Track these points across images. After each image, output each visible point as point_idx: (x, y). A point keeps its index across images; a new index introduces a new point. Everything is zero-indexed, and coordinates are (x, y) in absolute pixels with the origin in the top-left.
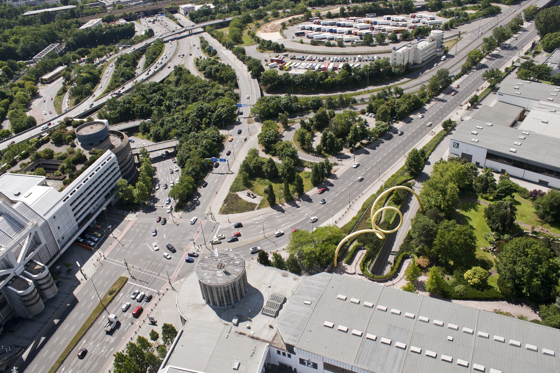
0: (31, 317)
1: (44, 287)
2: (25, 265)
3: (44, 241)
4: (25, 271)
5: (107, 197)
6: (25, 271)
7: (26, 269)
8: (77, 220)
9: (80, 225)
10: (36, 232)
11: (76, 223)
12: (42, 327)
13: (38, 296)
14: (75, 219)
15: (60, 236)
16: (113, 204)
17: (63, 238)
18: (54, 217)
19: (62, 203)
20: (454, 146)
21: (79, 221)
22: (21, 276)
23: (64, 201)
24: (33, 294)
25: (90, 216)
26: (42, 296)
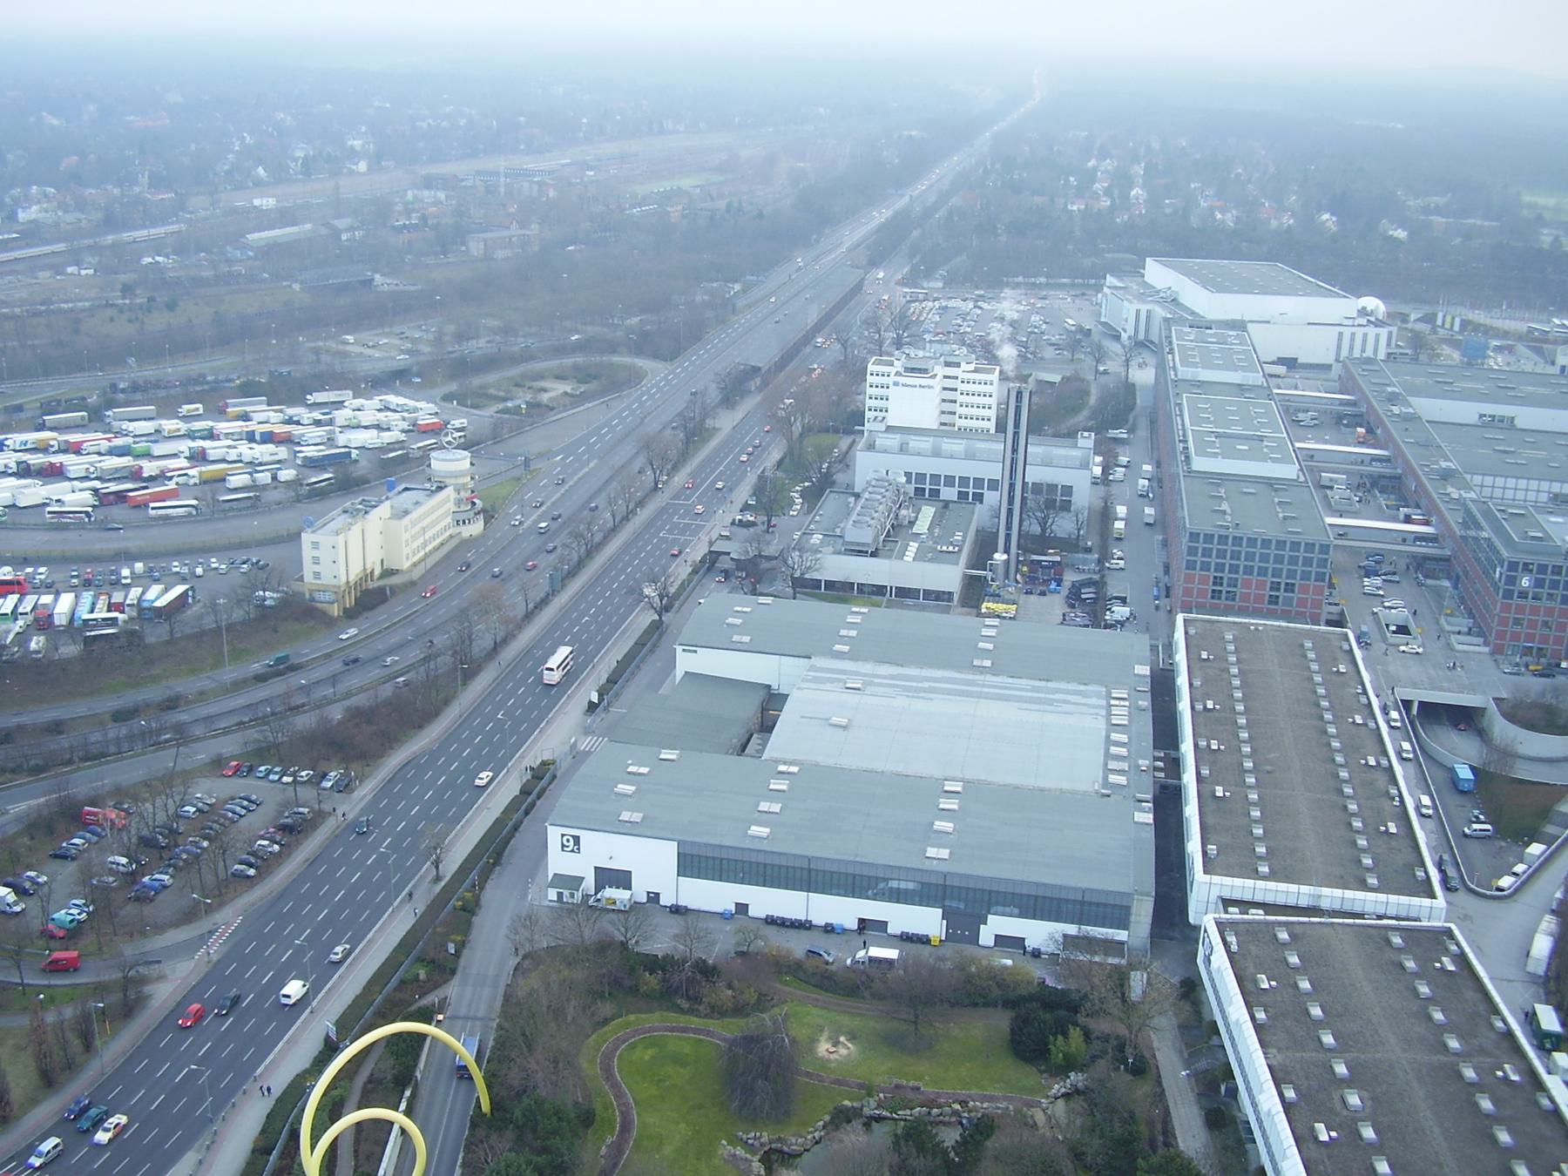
20: (563, 846)
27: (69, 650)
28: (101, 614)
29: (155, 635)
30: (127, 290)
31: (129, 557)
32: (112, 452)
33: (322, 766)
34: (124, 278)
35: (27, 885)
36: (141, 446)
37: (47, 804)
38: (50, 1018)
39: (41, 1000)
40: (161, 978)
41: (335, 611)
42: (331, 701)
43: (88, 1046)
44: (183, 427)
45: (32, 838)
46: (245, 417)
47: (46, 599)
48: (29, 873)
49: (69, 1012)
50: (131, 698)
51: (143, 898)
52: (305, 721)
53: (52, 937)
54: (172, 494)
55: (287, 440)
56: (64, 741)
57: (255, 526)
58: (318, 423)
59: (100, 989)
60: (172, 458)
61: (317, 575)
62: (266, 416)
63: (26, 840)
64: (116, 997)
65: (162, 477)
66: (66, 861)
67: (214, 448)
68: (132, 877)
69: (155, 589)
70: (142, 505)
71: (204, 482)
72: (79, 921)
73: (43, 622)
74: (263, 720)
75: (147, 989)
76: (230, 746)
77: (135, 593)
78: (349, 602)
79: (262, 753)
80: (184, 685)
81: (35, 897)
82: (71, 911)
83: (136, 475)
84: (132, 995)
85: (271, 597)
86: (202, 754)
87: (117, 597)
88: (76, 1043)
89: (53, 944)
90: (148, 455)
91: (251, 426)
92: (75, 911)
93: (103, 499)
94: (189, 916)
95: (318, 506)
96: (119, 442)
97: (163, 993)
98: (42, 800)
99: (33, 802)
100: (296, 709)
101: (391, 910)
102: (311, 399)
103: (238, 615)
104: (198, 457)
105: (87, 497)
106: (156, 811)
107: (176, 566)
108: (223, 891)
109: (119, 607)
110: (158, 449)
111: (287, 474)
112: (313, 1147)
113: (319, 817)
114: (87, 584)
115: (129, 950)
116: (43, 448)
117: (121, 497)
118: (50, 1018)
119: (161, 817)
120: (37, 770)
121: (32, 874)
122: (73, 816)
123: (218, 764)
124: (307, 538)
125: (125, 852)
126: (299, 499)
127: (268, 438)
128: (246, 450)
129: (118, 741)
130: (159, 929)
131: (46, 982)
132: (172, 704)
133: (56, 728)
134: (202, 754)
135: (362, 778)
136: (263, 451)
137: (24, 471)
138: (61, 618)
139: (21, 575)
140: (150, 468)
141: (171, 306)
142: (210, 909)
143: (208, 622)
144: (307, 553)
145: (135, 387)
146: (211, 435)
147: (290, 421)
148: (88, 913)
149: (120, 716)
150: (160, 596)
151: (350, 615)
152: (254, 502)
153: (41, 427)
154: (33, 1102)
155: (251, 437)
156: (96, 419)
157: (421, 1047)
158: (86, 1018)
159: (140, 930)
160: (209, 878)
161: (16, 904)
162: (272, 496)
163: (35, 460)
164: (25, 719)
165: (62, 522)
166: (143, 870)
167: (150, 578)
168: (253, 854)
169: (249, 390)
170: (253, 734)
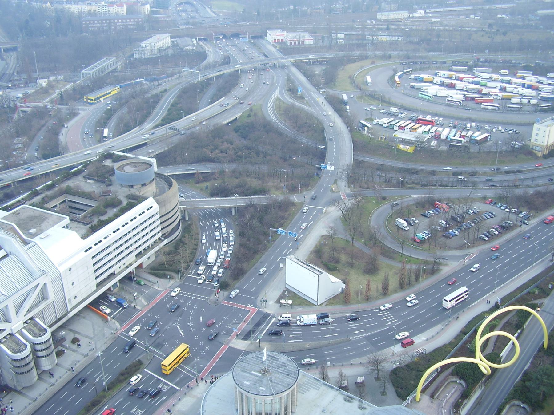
0: (19, 389)
1: (41, 354)
2: (25, 322)
3: (52, 297)
4: (23, 330)
5: (139, 255)
6: (23, 330)
7: (24, 327)
8: (96, 279)
9: (100, 285)
10: (45, 284)
11: (95, 282)
12: (30, 404)
13: (33, 363)
17: (75, 297)
18: (70, 269)
21: (99, 280)
22: (17, 335)
23: (86, 251)
24: (28, 360)
25: (113, 275)
26: (37, 366)
27: (444, 148)
28: (457, 138)
29: (474, 149)
30: (490, 26)
31: (471, 120)
32: (473, 83)
33: (521, 209)
34: (490, 21)
35: (412, 222)
36: (483, 82)
37: (424, 197)
38: (408, 267)
39: (406, 260)
40: (446, 265)
41: (540, 154)
42: (530, 187)
43: (417, 280)
44: (500, 78)
45: (417, 207)
46: (523, 78)
47: (440, 129)
48: (413, 218)
49: (414, 267)
50: (460, 169)
51: (447, 237)
52: (519, 191)
53: (415, 241)
54: (491, 101)
55: (537, 89)
56: (435, 178)
57: (517, 118)
58: (549, 84)
59: (426, 263)
60: (493, 87)
61: (536, 140)
62: (531, 79)
63: (415, 207)
64: (430, 267)
65: (488, 94)
66: (425, 218)
67: (509, 87)
68: (446, 229)
69: (478, 133)
70: (480, 103)
71: (503, 99)
72: (425, 238)
73: (437, 137)
74: (504, 187)
75: (441, 267)
76: (490, 193)
77: (470, 133)
78: (546, 152)
79: (501, 199)
80: (479, 169)
81: (413, 227)
82: (423, 234)
83: (479, 92)
84: (435, 267)
85: (517, 144)
86: (480, 194)
87: (464, 133)
88: (413, 277)
89: (415, 243)
90: (485, 86)
91: (524, 82)
92: (424, 235)
93: (466, 98)
94: (461, 247)
95: (542, 115)
96: (476, 79)
97: (446, 270)
98: (423, 196)
99: (420, 196)
100: (517, 186)
101: (532, 266)
102: (549, 75)
103: (504, 148)
104: (503, 89)
105: (461, 97)
106: (459, 209)
107: (486, 127)
108: (475, 242)
109: (464, 137)
110: (489, 84)
111: (534, 101)
112: (481, 338)
113: (515, 226)
114: (455, 127)
115: (439, 253)
116: (450, 78)
117: (473, 99)
118: (408, 267)
119: (461, 212)
120: (423, 185)
121: (414, 219)
122: (432, 203)
123: (484, 198)
124: (536, 126)
125: (446, 220)
126: (536, 111)
127: (530, 87)
128: (521, 90)
129: (452, 182)
130: (450, 248)
131: (409, 255)
132: (473, 174)
133: (433, 173)
134: (480, 194)
135: (534, 217)
136: (527, 91)
137: (442, 84)
138: (443, 137)
139: (433, 119)
140: (485, 90)
141: (505, 34)
142: (469, 247)
143: (493, 149)
144: (535, 131)
145: (486, 61)
146: (509, 82)
147: (539, 82)
148: (429, 237)
149: (455, 174)
150: (478, 136)
151: (545, 157)
152: (519, 109)
153: (451, 70)
154: (395, 292)
155: (523, 86)
156: (470, 70)
157: (528, 317)
158: (419, 270)
159: (444, 247)
160: (471, 237)
161: (406, 227)
162: (526, 108)
163: (447, 81)
164: (424, 168)
165: (451, 104)
166: (450, 227)
167: (477, 129)
168: (489, 233)
169: (526, 68)
170: (499, 191)
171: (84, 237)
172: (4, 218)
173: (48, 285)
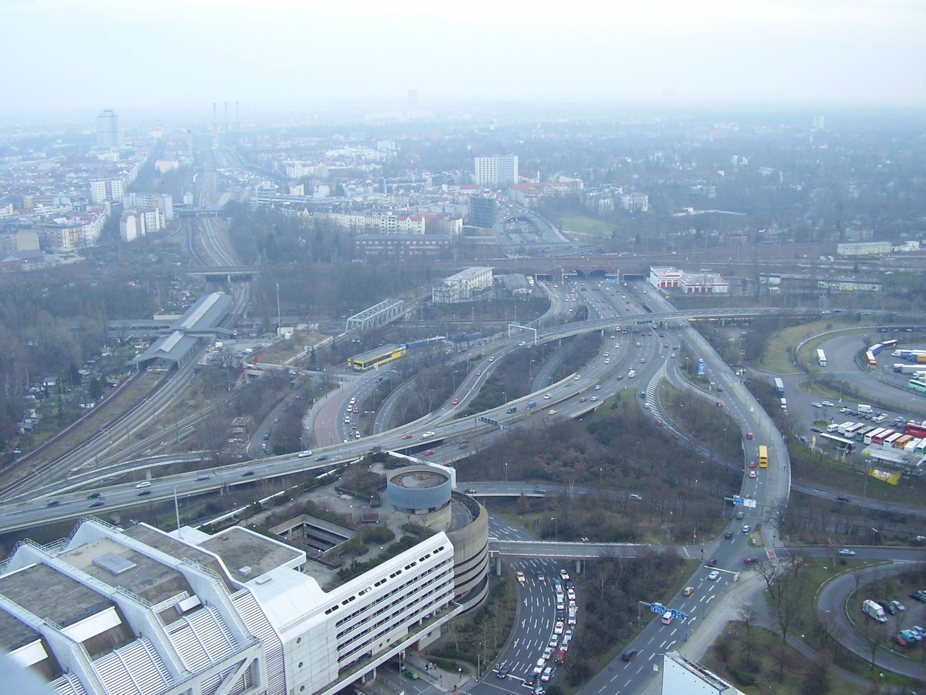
3: (264, 683)
5: (414, 628)
8: (339, 660)
9: (344, 672)
10: (256, 660)
11: (337, 667)
14: (337, 655)
15: (299, 683)
16: (421, 647)
18: (299, 639)
19: (323, 617)
23: (328, 612)
25: (367, 657)
35: (892, 608)
37: (916, 565)
39: (881, 677)
45: (902, 582)
48: (894, 602)
53: (898, 643)
63: (898, 582)
66: (917, 602)
72: (916, 640)
81: (894, 617)
82: (913, 632)
89: (897, 647)
92: (915, 633)
98: (914, 562)
99: (908, 562)
121: (897, 603)
131: (886, 667)
148: (923, 637)
161: (882, 616)
164: (916, 512)
171: (327, 589)
172: (204, 544)
173: (260, 662)
